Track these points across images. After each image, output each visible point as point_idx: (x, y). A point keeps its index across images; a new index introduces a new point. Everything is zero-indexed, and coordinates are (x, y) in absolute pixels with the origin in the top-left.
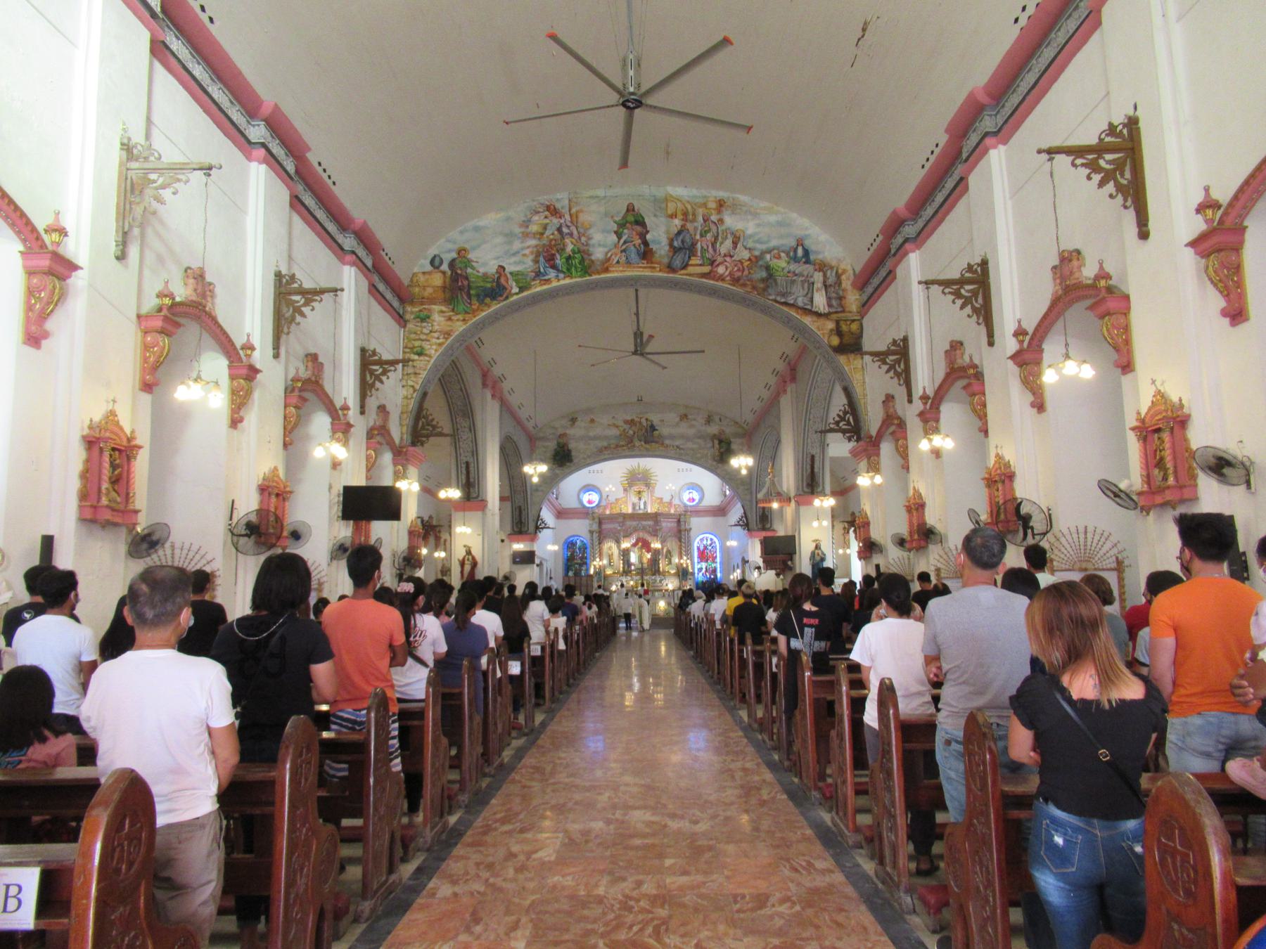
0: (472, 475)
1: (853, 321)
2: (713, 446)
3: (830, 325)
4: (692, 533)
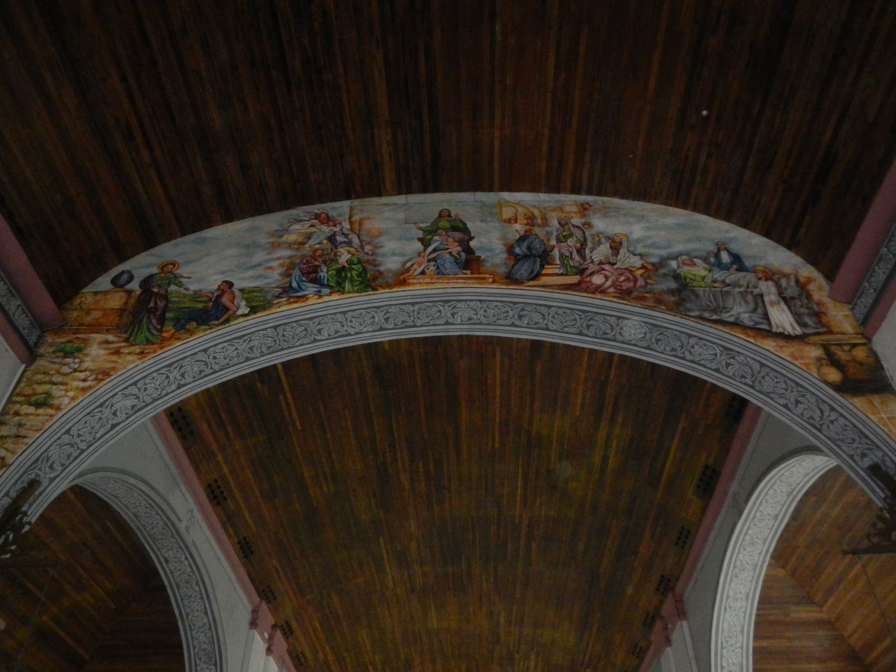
1: (854, 346)
3: (816, 352)
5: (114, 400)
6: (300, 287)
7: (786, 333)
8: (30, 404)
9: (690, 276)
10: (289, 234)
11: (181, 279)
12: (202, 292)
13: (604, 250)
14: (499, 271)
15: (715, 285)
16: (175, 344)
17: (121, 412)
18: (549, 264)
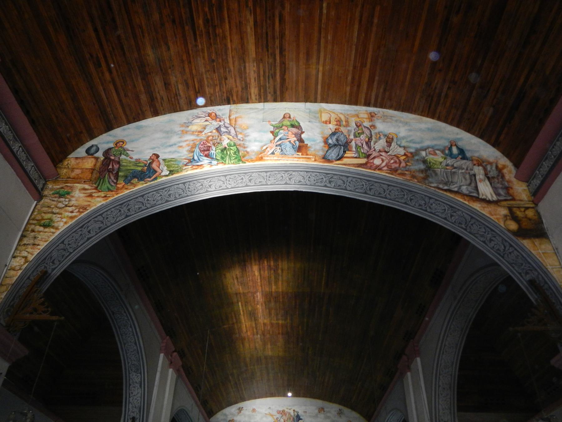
1: (527, 208)
3: (503, 211)
5: (89, 224)
6: (199, 160)
7: (487, 199)
8: (41, 226)
9: (433, 161)
10: (193, 125)
11: (128, 152)
12: (140, 160)
14: (319, 154)
15: (448, 167)
16: (125, 192)
17: (93, 230)
18: (349, 150)
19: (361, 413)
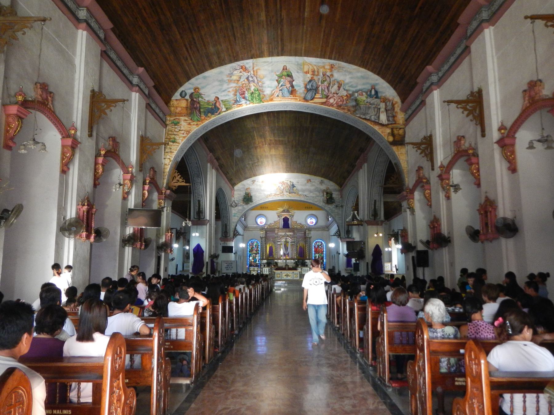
0: (201, 207)
1: (400, 128)
2: (323, 196)
3: (388, 131)
4: (312, 239)
13: (336, 87)
19: (336, 183)
